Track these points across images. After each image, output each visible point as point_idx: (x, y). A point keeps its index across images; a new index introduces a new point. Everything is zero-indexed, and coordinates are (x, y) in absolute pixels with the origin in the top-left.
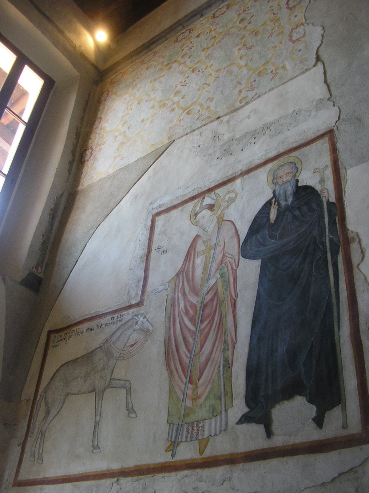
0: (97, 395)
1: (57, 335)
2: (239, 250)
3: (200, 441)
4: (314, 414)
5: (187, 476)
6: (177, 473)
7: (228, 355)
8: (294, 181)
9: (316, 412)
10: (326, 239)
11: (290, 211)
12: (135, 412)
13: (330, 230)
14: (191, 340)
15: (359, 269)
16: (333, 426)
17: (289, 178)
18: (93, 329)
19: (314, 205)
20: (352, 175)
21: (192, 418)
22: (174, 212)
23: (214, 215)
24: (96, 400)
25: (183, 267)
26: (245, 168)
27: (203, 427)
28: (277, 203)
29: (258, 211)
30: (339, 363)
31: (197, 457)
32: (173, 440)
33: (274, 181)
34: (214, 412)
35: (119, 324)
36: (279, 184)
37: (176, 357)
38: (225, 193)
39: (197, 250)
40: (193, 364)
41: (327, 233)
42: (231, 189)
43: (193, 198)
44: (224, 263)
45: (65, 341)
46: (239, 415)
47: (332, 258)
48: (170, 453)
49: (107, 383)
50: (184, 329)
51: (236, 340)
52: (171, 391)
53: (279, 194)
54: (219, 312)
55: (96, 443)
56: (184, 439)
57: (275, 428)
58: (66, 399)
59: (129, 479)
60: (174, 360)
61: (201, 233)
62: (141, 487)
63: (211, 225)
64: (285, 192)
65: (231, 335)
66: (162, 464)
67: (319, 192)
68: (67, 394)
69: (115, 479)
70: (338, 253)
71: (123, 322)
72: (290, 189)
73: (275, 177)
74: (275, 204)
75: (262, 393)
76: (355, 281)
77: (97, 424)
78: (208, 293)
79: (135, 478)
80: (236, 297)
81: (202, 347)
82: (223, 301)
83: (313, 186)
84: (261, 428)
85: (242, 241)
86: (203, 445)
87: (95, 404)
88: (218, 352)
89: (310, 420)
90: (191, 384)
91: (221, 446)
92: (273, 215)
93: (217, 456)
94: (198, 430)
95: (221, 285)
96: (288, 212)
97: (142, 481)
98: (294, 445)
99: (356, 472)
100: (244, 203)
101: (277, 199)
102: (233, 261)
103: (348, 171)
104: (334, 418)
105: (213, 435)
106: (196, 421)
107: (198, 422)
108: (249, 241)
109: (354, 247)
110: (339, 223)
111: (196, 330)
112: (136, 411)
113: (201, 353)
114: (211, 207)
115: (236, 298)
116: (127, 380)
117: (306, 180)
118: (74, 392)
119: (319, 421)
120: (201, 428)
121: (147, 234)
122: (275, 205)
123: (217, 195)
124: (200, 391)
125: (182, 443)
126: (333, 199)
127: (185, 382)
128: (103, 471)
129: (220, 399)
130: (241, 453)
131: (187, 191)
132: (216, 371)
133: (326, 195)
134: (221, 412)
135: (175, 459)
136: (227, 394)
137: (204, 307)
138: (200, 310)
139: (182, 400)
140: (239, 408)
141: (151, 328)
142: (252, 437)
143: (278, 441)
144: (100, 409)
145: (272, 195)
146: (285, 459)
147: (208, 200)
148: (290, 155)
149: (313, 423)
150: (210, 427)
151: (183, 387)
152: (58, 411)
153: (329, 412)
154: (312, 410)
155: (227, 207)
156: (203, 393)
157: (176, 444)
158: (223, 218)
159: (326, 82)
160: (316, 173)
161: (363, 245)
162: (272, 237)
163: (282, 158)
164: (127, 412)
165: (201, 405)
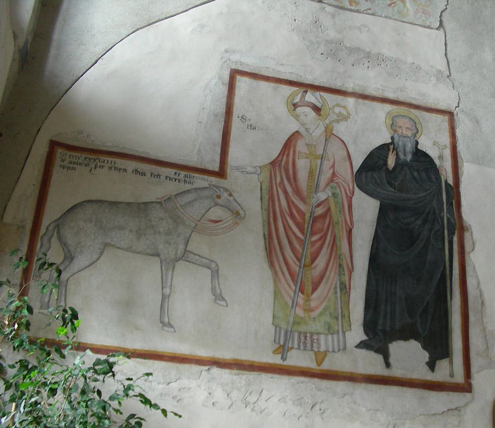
0: (164, 263)
1: (69, 153)
2: (352, 177)
3: (316, 353)
4: (427, 360)
5: (302, 382)
6: (291, 377)
7: (345, 280)
8: (414, 141)
9: (429, 358)
10: (444, 216)
11: (409, 169)
12: (224, 299)
13: (447, 209)
14: (298, 246)
15: (469, 257)
16: (442, 372)
17: (409, 133)
18: (143, 174)
19: (433, 177)
20: (467, 169)
21: (303, 328)
22: (263, 84)
23: (321, 120)
24: (163, 268)
25: (280, 158)
26: (358, 90)
27: (318, 340)
28: (395, 152)
29: (375, 148)
30: (450, 326)
31: (314, 367)
32: (282, 343)
33: (393, 126)
34: (330, 330)
35: (188, 187)
36: (398, 133)
37: (281, 259)
38: (335, 103)
39: (298, 149)
40: (304, 273)
41: (445, 210)
42: (343, 104)
43: (291, 83)
44: (336, 183)
45: (88, 169)
46: (358, 341)
47: (449, 235)
48: (280, 356)
49: (179, 252)
50: (290, 233)
51: (353, 268)
52: (277, 294)
53: (398, 144)
54: (332, 232)
55: (166, 320)
56: (296, 346)
57: (392, 360)
58: (106, 251)
59: (227, 371)
60: (278, 261)
61: (302, 131)
62: (244, 382)
63: (316, 131)
64: (404, 146)
65: (346, 260)
66: (270, 364)
67: (438, 167)
68: (107, 245)
69: (207, 368)
70: (454, 234)
71: (196, 186)
72: (409, 147)
73: (394, 123)
74: (393, 152)
75: (379, 327)
76: (466, 264)
77: (165, 298)
78: (318, 205)
79: (235, 371)
80: (351, 224)
81: (313, 261)
82: (337, 223)
83: (432, 157)
84: (380, 358)
85: (356, 169)
86: (320, 357)
87: (162, 273)
88: (333, 274)
89: (424, 363)
90: (302, 292)
91: (338, 363)
92: (391, 162)
93: (337, 372)
94: (312, 342)
95: (334, 205)
96: (406, 168)
97: (244, 377)
98: (411, 379)
99: (459, 411)
100: (358, 130)
101: (395, 147)
102: (346, 185)
103: (464, 163)
104: (443, 365)
105: (331, 350)
106: (310, 333)
107: (312, 334)
108: (364, 174)
109: (467, 235)
110: (455, 205)
111: (306, 238)
112: (227, 299)
113: (313, 266)
114: (317, 109)
115: (351, 227)
116: (213, 261)
117: (426, 147)
118: (119, 246)
119: (431, 365)
120: (315, 341)
121: (224, 90)
122: (393, 153)
123: (322, 98)
124: (313, 304)
125: (293, 350)
126: (451, 181)
127: (294, 290)
128: (185, 355)
129: (337, 319)
130: (361, 374)
131: (280, 68)
132: (332, 291)
133: (444, 174)
134: (338, 332)
135: (285, 363)
136: (345, 316)
137: (315, 219)
138: (309, 220)
139: (291, 306)
140: (357, 334)
141: (241, 212)
142: (370, 363)
143: (397, 371)
144: (169, 280)
145: (390, 141)
146: (405, 389)
147: (310, 97)
148: (413, 111)
149: (426, 365)
150: (325, 342)
151: (292, 294)
152: (91, 261)
153: (440, 361)
154: (425, 356)
155: (338, 121)
156: (317, 308)
157: (286, 350)
158: (331, 132)
159: (446, 55)
160: (435, 146)
161: (474, 238)
162: (391, 185)
163: (402, 108)
164: (214, 297)
165: (314, 318)
